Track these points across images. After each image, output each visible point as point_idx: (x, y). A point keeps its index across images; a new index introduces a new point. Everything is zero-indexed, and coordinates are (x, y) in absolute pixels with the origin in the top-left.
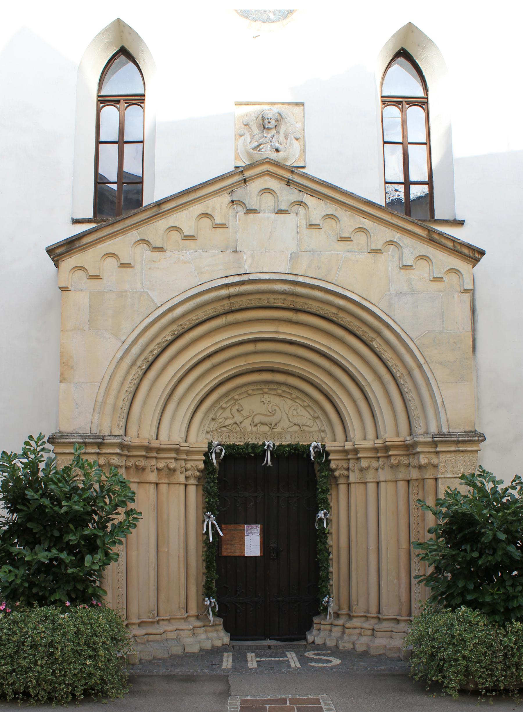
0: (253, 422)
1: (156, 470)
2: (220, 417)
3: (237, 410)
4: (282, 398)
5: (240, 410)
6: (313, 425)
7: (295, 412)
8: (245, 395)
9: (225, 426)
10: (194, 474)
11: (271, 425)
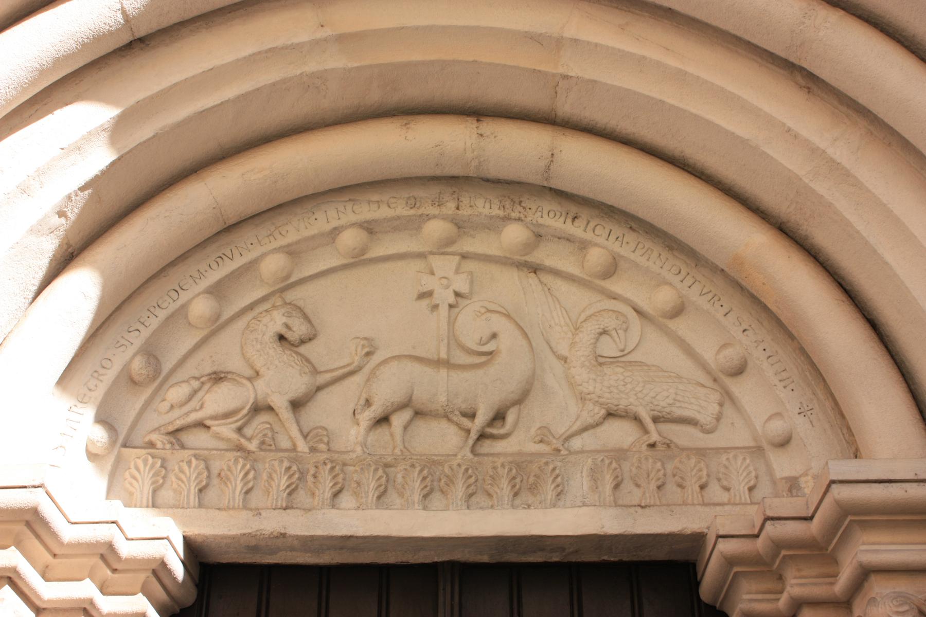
0: (368, 403)
2: (180, 375)
3: (281, 338)
4: (532, 279)
5: (292, 336)
6: (718, 419)
7: (608, 348)
9: (201, 425)
11: (472, 416)
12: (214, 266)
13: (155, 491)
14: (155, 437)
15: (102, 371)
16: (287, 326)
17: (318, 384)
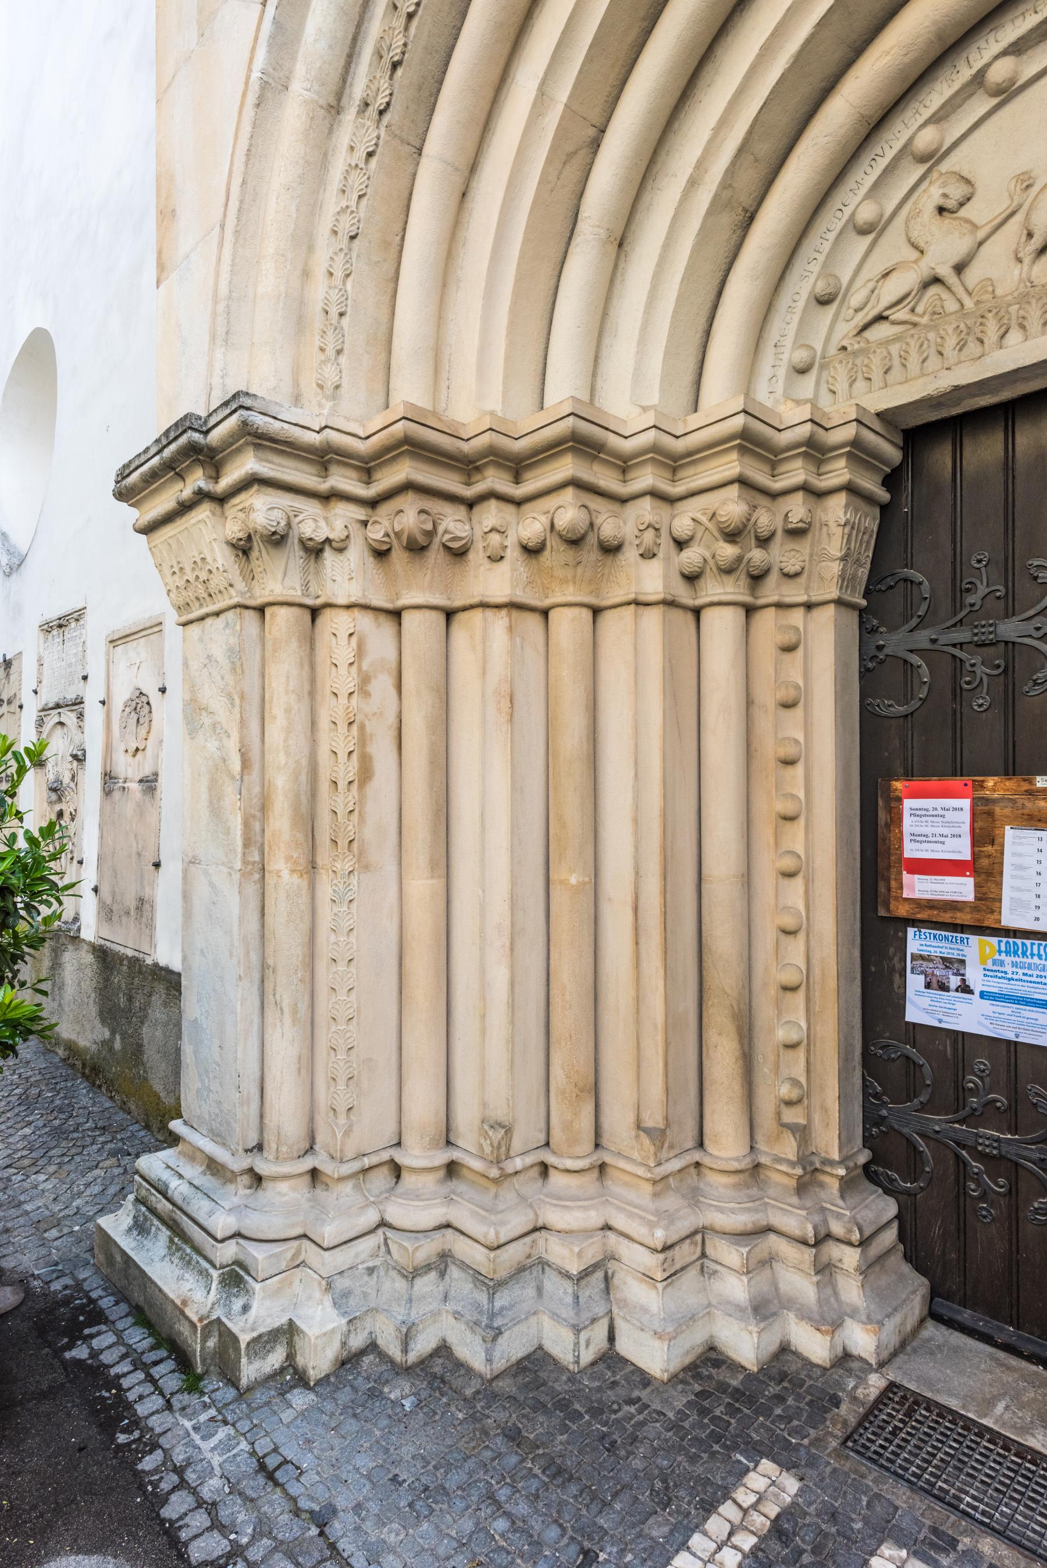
1: (513, 554)
5: (950, 204)
8: (981, 105)
9: (880, 318)
10: (713, 557)
12: (869, 170)
13: (851, 386)
14: (845, 343)
15: (794, 305)
16: (945, 196)
17: (979, 239)
